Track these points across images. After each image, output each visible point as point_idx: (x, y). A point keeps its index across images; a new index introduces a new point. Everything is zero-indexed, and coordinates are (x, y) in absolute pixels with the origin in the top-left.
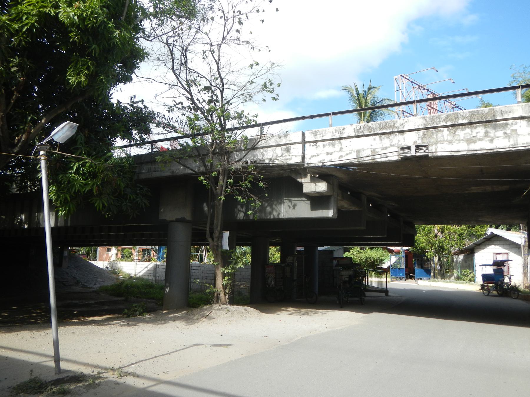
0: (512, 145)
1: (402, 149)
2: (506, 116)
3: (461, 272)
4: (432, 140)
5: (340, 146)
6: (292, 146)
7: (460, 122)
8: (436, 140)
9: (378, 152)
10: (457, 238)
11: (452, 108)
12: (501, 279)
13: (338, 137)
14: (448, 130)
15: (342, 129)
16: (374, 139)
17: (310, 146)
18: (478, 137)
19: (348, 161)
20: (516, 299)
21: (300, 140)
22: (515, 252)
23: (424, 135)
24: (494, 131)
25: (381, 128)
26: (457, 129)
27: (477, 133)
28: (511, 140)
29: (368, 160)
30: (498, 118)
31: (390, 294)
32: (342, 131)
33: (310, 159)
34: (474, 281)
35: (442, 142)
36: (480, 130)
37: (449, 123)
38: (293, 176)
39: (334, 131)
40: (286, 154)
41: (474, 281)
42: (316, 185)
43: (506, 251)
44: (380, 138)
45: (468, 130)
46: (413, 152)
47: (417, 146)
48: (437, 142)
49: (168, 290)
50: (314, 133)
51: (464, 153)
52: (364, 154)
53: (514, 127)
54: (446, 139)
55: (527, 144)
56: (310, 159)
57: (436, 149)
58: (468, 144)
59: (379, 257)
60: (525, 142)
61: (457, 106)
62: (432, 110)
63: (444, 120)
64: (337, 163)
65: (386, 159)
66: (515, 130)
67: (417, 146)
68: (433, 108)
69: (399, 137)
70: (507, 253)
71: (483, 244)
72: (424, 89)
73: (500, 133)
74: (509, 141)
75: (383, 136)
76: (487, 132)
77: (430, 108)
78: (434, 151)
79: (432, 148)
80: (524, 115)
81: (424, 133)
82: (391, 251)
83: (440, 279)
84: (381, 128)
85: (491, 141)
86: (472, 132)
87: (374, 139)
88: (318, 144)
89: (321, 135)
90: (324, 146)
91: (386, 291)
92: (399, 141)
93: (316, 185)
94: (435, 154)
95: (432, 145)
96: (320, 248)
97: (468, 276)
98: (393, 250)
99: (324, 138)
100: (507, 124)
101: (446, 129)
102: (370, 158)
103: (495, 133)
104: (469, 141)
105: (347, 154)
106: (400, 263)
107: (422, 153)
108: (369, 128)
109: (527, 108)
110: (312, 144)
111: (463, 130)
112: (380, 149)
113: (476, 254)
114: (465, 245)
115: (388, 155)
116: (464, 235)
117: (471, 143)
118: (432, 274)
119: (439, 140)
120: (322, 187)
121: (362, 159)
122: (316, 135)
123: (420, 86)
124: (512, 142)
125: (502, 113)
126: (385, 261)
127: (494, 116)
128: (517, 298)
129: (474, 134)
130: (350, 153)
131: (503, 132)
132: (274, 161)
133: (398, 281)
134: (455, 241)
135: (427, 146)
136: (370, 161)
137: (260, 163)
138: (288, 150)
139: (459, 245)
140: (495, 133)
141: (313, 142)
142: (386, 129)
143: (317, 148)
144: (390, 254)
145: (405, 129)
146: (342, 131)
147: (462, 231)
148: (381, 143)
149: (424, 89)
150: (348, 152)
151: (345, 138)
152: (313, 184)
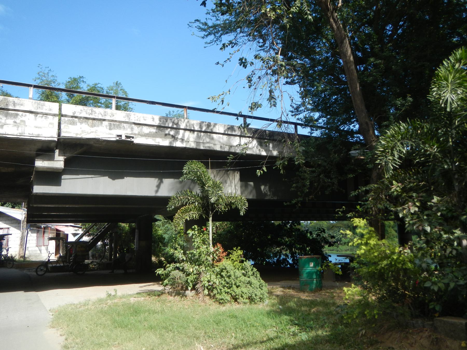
0: (20, 133)
2: (17, 108)
20: (10, 268)
22: (15, 227)
24: (5, 118)
28: (20, 128)
30: (10, 107)
43: (8, 226)
53: (23, 118)
55: (32, 134)
70: (8, 228)
73: (10, 121)
74: (18, 130)
80: (33, 110)
100: (17, 115)
103: (5, 120)
109: (36, 105)
125: (14, 104)
128: (12, 268)
131: (13, 120)
140: (5, 120)
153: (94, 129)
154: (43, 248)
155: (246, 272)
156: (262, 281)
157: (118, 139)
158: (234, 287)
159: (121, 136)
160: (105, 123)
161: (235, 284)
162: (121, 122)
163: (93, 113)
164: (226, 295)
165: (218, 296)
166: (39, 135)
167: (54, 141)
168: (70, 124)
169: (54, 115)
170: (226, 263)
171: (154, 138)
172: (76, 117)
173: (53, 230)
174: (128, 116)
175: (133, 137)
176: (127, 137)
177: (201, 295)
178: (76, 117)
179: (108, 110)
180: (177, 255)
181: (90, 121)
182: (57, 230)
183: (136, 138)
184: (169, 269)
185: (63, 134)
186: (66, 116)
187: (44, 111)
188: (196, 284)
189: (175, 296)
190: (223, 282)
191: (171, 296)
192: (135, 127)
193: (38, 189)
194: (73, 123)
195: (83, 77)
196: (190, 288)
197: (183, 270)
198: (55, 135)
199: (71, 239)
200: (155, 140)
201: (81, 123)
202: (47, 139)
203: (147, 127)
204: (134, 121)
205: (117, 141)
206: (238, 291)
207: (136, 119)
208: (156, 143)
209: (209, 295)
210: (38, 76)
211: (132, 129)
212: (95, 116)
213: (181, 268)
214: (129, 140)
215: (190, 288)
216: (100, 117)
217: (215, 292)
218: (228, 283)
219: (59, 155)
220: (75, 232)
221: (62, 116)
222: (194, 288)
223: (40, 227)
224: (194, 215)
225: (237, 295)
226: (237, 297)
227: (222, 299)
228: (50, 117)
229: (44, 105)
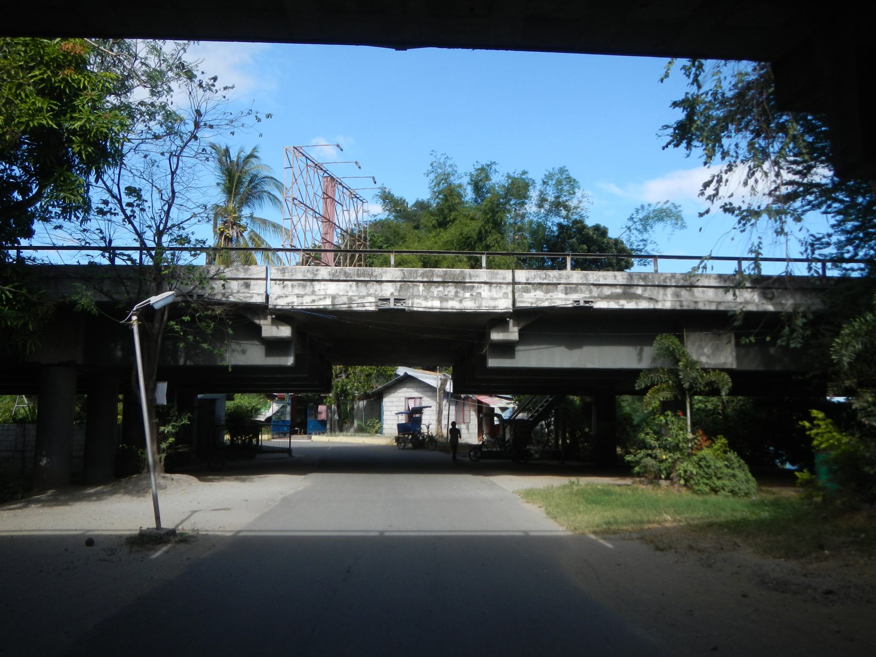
0: (477, 307)
1: (380, 300)
3: (366, 423)
4: (408, 294)
5: (312, 289)
6: (253, 282)
7: (435, 279)
8: (413, 295)
9: (354, 300)
10: (364, 379)
11: (352, 198)
12: (418, 429)
13: (311, 278)
14: (423, 286)
15: (315, 270)
16: (351, 286)
17: (276, 284)
18: (449, 296)
19: (322, 307)
23: (401, 287)
25: (358, 275)
26: (432, 286)
27: (449, 292)
29: (344, 307)
31: (294, 454)
32: (316, 272)
33: (276, 299)
34: (381, 433)
35: (419, 297)
36: (451, 290)
37: (425, 279)
38: (249, 316)
39: (306, 271)
40: (245, 290)
41: (381, 433)
42: (278, 328)
44: (357, 285)
45: (441, 288)
46: (391, 305)
47: (395, 299)
48: (413, 297)
50: (281, 270)
51: (438, 310)
52: (339, 301)
54: (421, 294)
56: (276, 299)
57: (412, 304)
58: (441, 302)
59: (254, 406)
60: (487, 305)
61: (358, 196)
62: (328, 200)
63: (421, 275)
64: (309, 307)
65: (364, 309)
66: (480, 294)
67: (395, 299)
68: (330, 197)
69: (376, 286)
72: (322, 169)
73: (468, 295)
74: (475, 303)
75: (360, 284)
76: (457, 292)
77: (326, 196)
78: (410, 305)
79: (409, 303)
80: (488, 281)
81: (401, 285)
82: (273, 398)
85: (461, 301)
86: (444, 290)
87: (351, 286)
88: (286, 283)
89: (290, 274)
90: (292, 286)
91: (288, 450)
92: (376, 291)
93: (278, 328)
94: (411, 309)
95: (409, 299)
96: (200, 396)
97: (374, 427)
98: (276, 396)
99: (294, 278)
100: (473, 287)
101: (421, 284)
102: (346, 306)
104: (443, 299)
105: (320, 299)
107: (399, 306)
108: (345, 273)
110: (278, 282)
111: (437, 287)
112: (357, 297)
113: (385, 400)
114: (372, 388)
115: (367, 304)
116: (373, 375)
117: (444, 301)
118: (328, 426)
119: (415, 294)
120: (285, 331)
121: (338, 306)
122: (284, 273)
123: (316, 165)
124: (477, 305)
125: (470, 276)
126: (262, 410)
127: (464, 278)
129: (446, 293)
130: (325, 298)
132: (228, 297)
133: (280, 438)
134: (361, 383)
135: (404, 299)
136: (347, 309)
137: (209, 299)
138: (247, 286)
139: (366, 388)
141: (280, 280)
142: (364, 277)
143: (284, 287)
144: (269, 401)
145: (383, 279)
146: (316, 272)
147: (371, 371)
148: (358, 291)
149: (322, 169)
150: (322, 297)
151: (318, 280)
152: (274, 328)
153: (548, 296)
155: (731, 464)
156: (750, 475)
157: (575, 305)
158: (714, 479)
159: (579, 301)
160: (561, 287)
161: (716, 475)
162: (577, 284)
163: (547, 277)
164: (704, 486)
166: (495, 307)
167: (510, 312)
168: (525, 292)
169: (508, 284)
170: (706, 452)
171: (617, 300)
172: (529, 284)
173: (473, 401)
174: (585, 276)
175: (592, 302)
176: (586, 302)
177: (676, 486)
178: (529, 284)
179: (563, 272)
180: (649, 440)
181: (545, 286)
182: (479, 402)
183: (596, 302)
184: (640, 456)
185: (518, 304)
186: (519, 283)
187: (498, 281)
188: (670, 473)
189: (647, 485)
190: (702, 473)
191: (644, 485)
192: (594, 289)
193: (493, 363)
195: (495, 163)
196: (663, 477)
197: (655, 458)
198: (511, 306)
200: (618, 302)
201: (535, 290)
202: (503, 311)
203: (608, 287)
204: (592, 282)
205: (574, 308)
206: (719, 483)
207: (595, 278)
208: (620, 306)
209: (685, 485)
210: (430, 168)
211: (591, 291)
212: (550, 281)
213: (653, 455)
215: (663, 477)
216: (555, 281)
217: (692, 482)
218: (707, 474)
219: (514, 326)
220: (502, 406)
221: (516, 283)
222: (668, 478)
223: (460, 398)
224: (667, 395)
225: (717, 487)
226: (717, 489)
227: (700, 490)
228: (504, 286)
229: (497, 274)
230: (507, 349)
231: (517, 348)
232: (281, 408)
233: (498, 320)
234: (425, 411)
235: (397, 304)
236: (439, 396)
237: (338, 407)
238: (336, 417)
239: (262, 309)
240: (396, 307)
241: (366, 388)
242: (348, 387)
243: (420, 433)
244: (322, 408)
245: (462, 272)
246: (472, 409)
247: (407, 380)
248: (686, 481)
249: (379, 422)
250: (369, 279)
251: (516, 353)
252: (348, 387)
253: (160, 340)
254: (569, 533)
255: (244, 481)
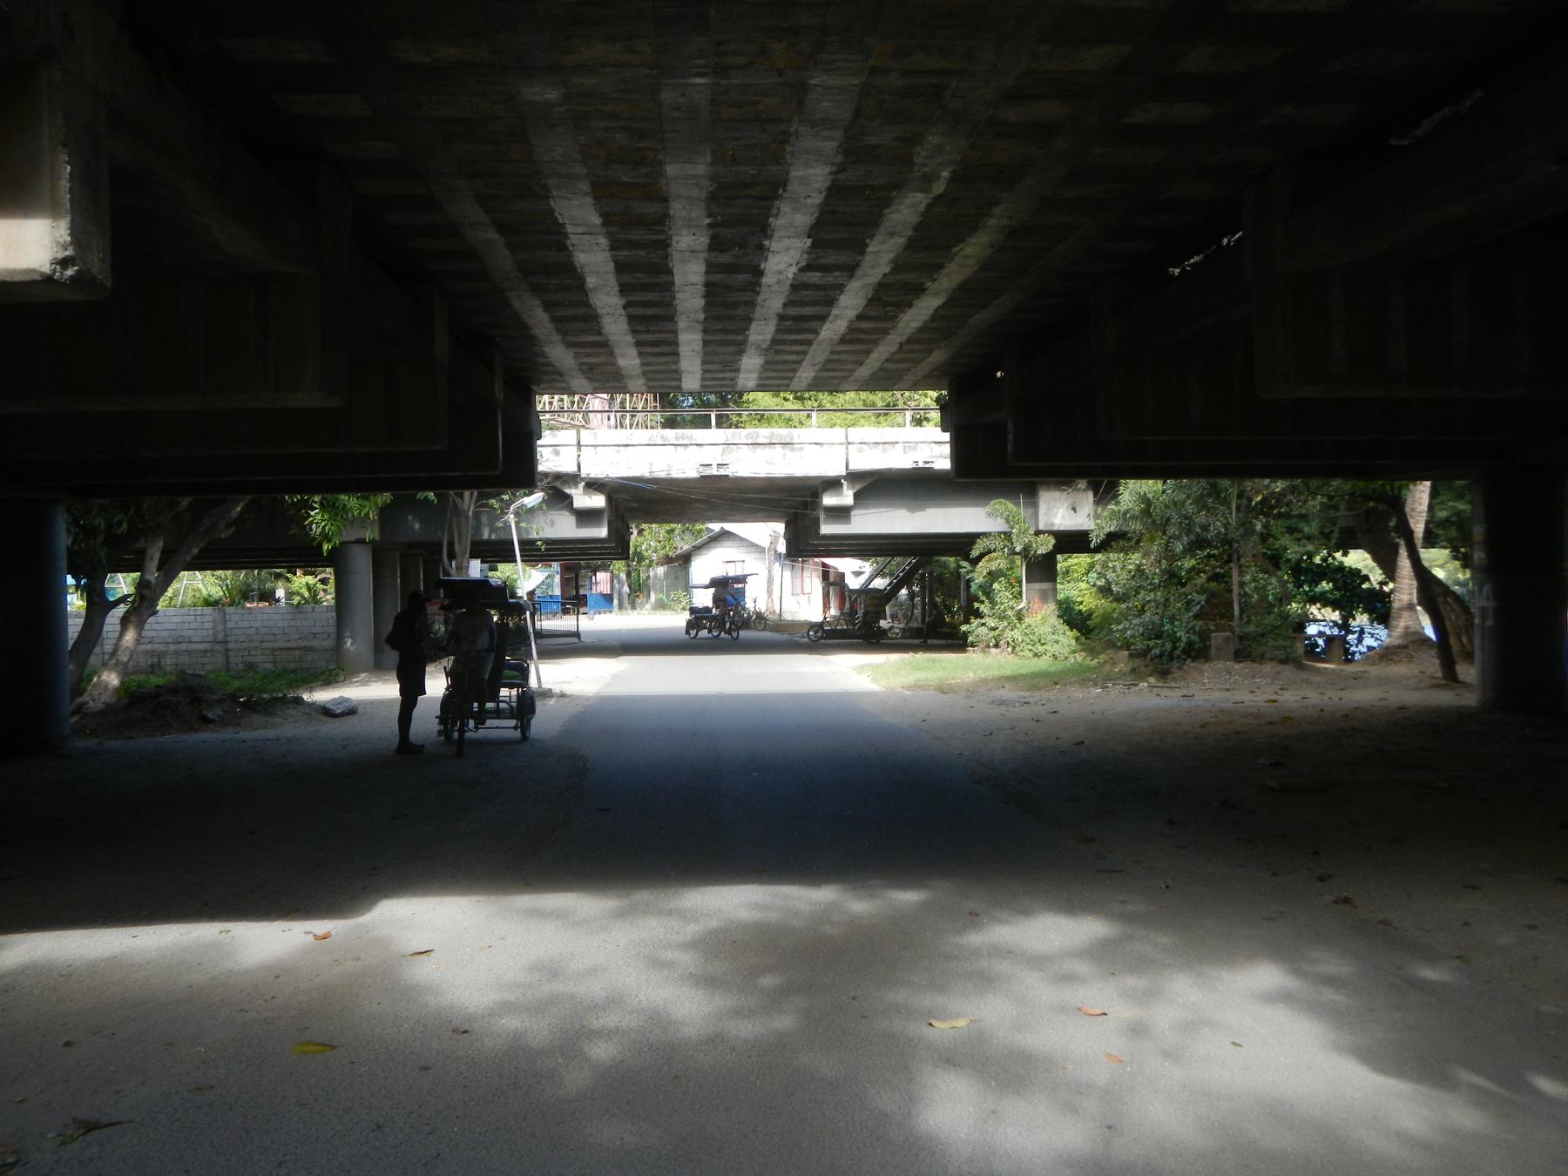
21: (575, 442)
23: (724, 450)
29: (663, 475)
37: (750, 441)
42: (590, 498)
43: (743, 557)
46: (714, 471)
49: (349, 644)
67: (718, 465)
71: (707, 545)
75: (679, 447)
83: (629, 611)
84: (677, 438)
94: (736, 474)
100: (802, 448)
102: (666, 473)
106: (550, 586)
107: (722, 472)
108: (662, 437)
113: (693, 564)
116: (677, 532)
118: (616, 602)
120: (598, 501)
121: (656, 474)
134: (660, 542)
138: (557, 453)
141: (592, 446)
144: (528, 568)
152: (587, 498)
154: (803, 598)
160: (899, 447)
162: (917, 443)
165: (1021, 654)
172: (865, 443)
178: (865, 443)
182: (824, 565)
185: (851, 467)
186: (853, 443)
193: (827, 529)
194: (861, 451)
199: (854, 583)
206: (1041, 649)
214: (928, 466)
222: (997, 646)
230: (841, 513)
231: (852, 513)
232: (546, 578)
233: (833, 484)
234: (749, 579)
235: (720, 470)
236: (769, 558)
237: (629, 575)
238: (626, 589)
239: (573, 479)
240: (718, 474)
241: (667, 549)
242: (643, 548)
243: (744, 609)
244: (602, 576)
245: (790, 432)
246: (814, 574)
247: (724, 535)
248: (1014, 648)
249: (686, 595)
250: (688, 443)
251: (852, 517)
252: (643, 548)
253: (471, 513)
254: (884, 689)
255: (558, 663)
